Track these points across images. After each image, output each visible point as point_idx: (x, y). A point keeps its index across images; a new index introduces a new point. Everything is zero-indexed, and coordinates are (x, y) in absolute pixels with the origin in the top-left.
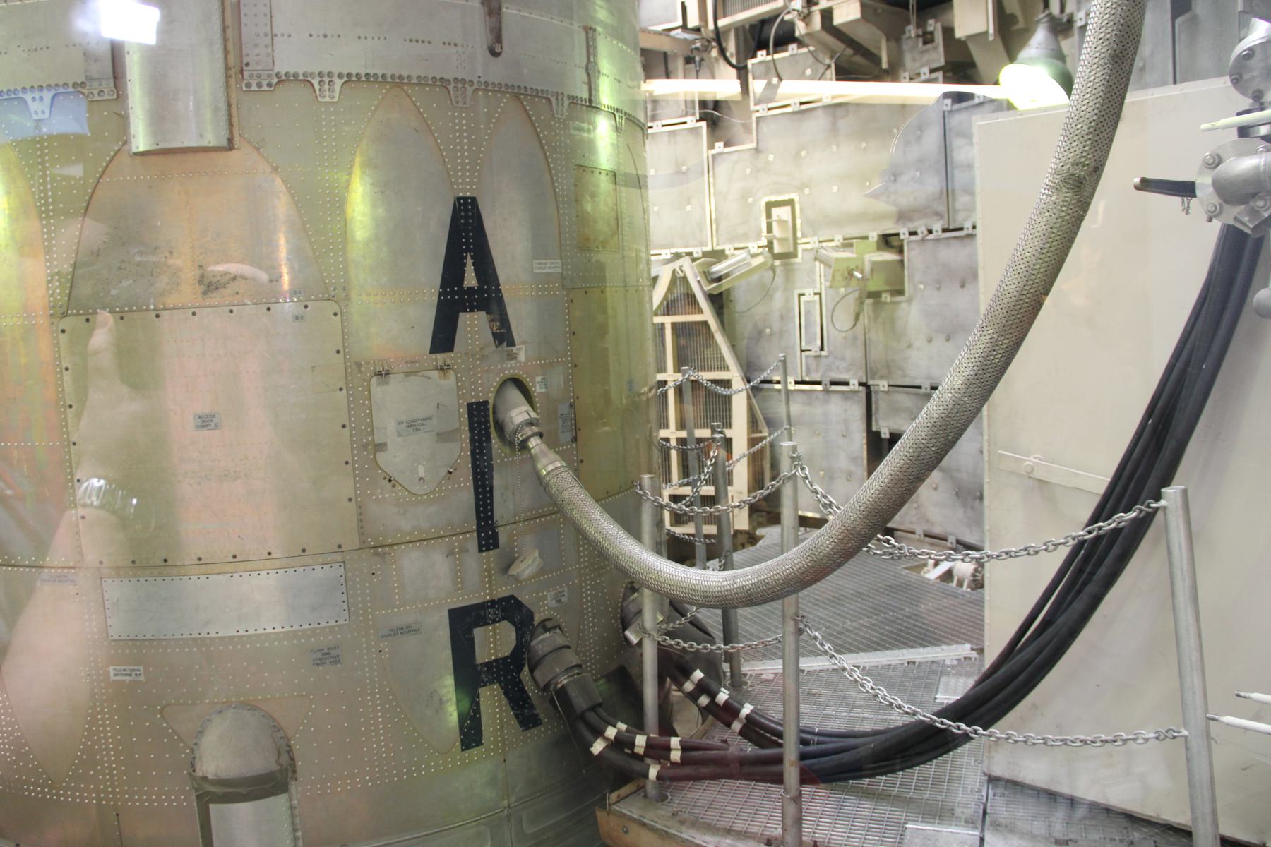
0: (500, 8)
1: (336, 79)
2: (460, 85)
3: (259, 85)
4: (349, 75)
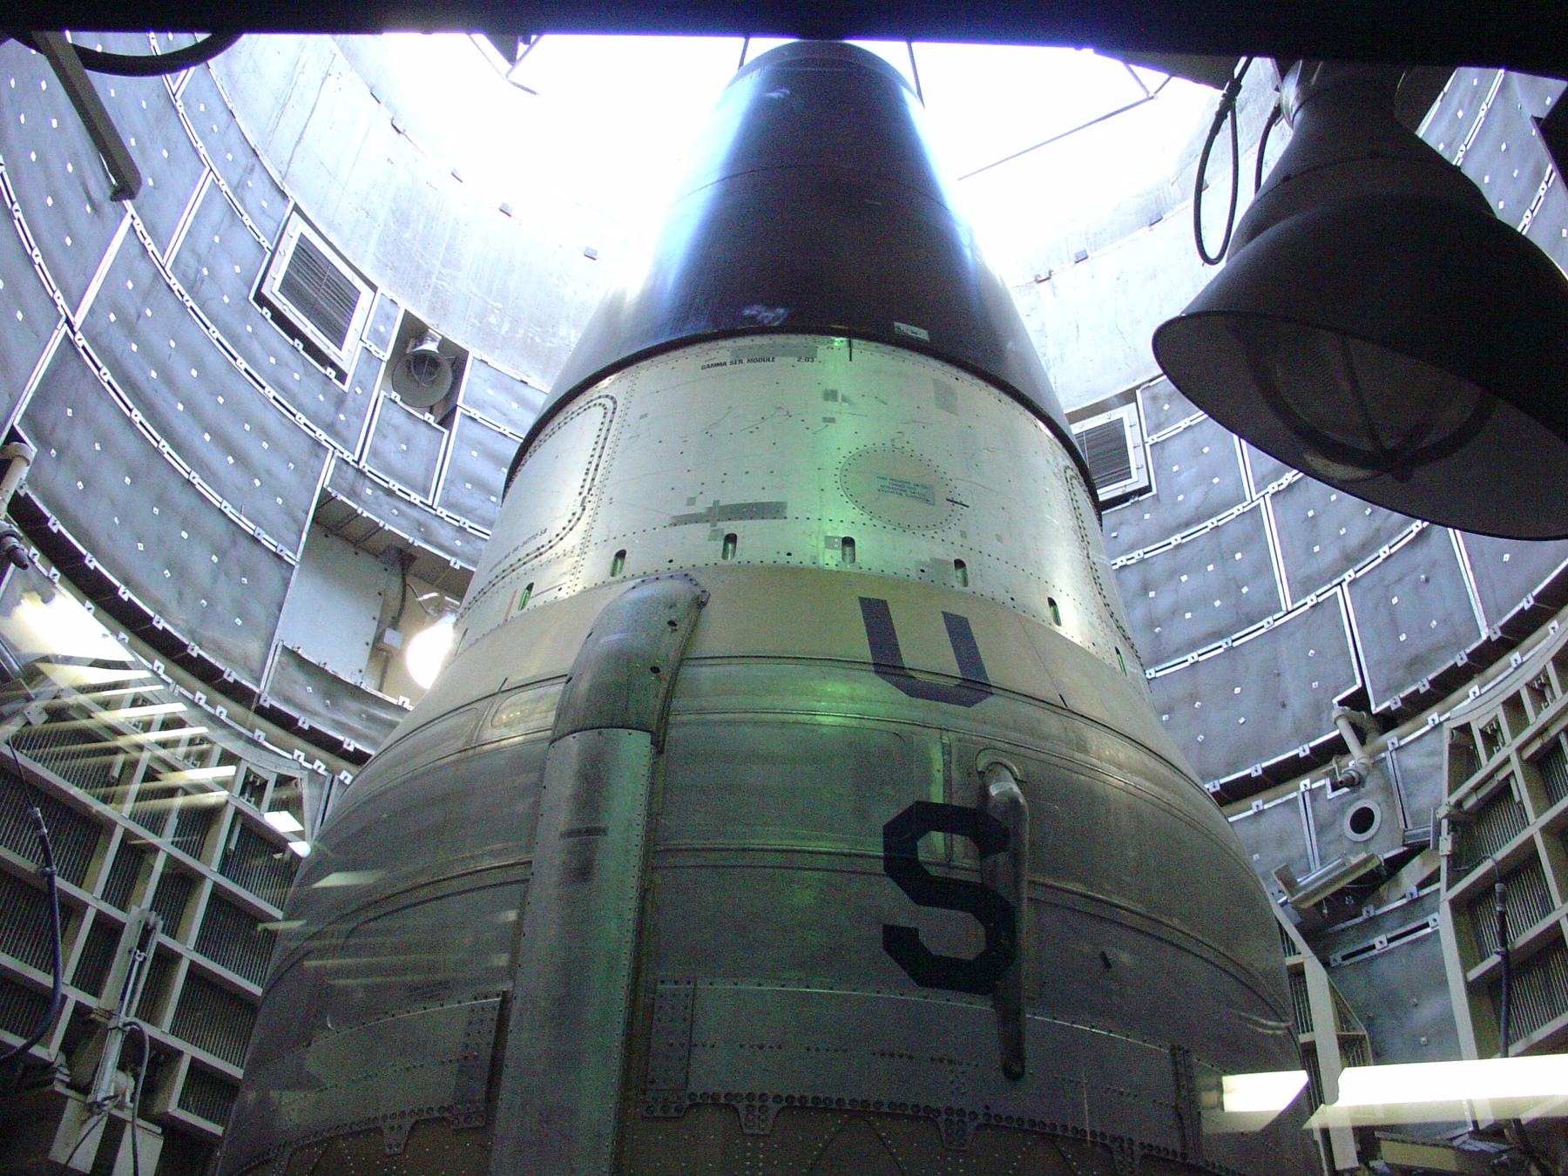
0: (1019, 1012)
1: (770, 1103)
2: (955, 1118)
3: (665, 1109)
4: (790, 1098)
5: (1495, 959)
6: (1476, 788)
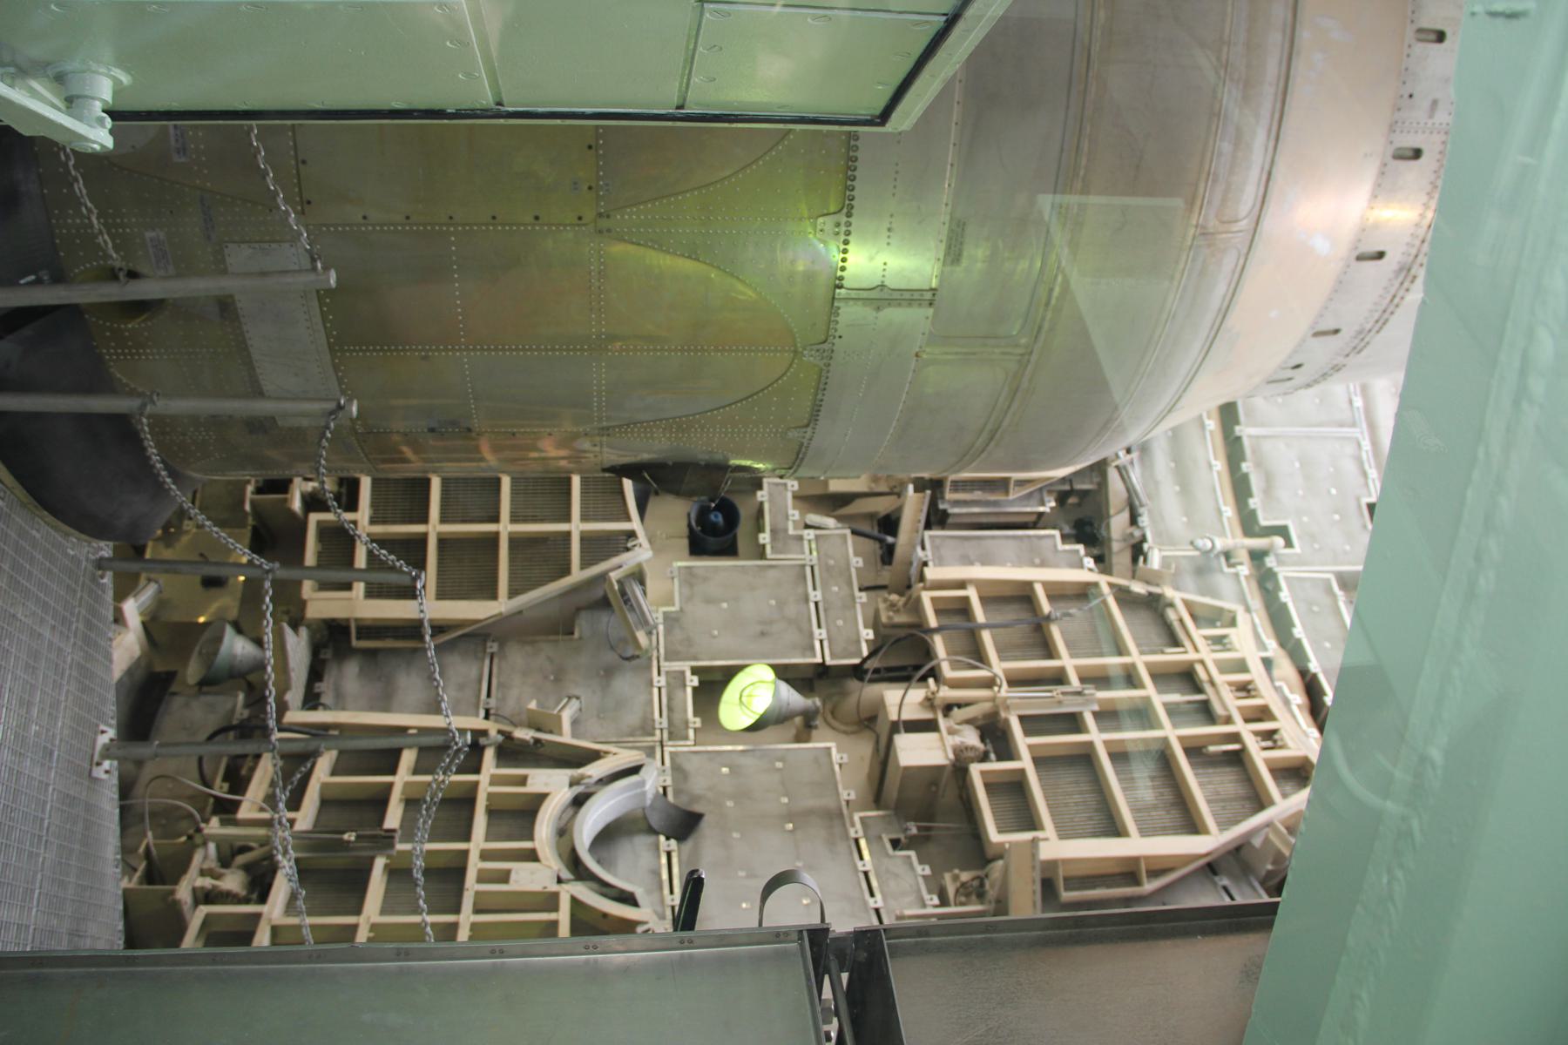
5: (1046, 607)
6: (1181, 621)
